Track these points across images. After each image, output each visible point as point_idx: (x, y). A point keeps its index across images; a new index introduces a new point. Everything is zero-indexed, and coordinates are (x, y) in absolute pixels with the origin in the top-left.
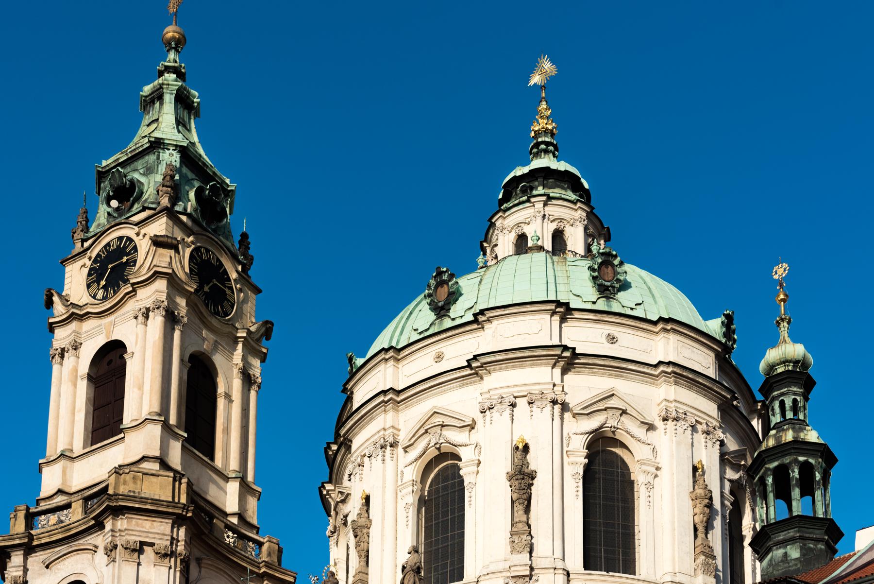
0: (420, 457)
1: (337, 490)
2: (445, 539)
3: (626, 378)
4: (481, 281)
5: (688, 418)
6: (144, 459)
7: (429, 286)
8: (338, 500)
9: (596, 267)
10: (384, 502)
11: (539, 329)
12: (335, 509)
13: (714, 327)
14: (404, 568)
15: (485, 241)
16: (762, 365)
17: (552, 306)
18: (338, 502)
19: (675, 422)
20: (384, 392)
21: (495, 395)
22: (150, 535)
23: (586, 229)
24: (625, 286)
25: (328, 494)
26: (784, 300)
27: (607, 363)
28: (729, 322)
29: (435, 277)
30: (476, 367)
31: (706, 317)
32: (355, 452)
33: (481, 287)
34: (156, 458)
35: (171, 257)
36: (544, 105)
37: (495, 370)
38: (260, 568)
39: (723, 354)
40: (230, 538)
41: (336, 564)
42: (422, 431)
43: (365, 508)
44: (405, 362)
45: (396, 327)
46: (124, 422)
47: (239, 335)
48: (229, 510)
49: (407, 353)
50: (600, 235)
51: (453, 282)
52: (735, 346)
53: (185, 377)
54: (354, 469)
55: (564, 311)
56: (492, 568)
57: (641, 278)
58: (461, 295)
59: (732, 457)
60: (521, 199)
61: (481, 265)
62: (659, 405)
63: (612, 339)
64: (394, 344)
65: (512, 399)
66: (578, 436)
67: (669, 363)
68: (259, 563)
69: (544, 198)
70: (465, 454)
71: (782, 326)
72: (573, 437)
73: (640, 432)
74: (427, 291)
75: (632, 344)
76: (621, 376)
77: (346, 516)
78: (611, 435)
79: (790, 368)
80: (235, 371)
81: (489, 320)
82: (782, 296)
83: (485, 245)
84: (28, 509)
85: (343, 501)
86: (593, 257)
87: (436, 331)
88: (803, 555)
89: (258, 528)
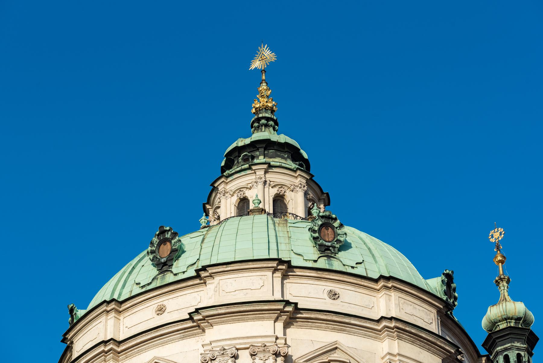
3: (349, 333)
4: (203, 239)
7: (152, 244)
9: (316, 228)
11: (261, 285)
13: (435, 285)
15: (208, 203)
16: (484, 322)
17: (274, 264)
20: (105, 342)
21: (217, 346)
23: (306, 194)
24: (345, 246)
26: (502, 262)
28: (449, 280)
29: (158, 235)
30: (198, 320)
31: (426, 277)
33: (204, 245)
36: (264, 86)
37: (217, 323)
39: (446, 311)
49: (128, 306)
50: (319, 200)
51: (175, 240)
52: (456, 303)
55: (286, 268)
57: (361, 239)
58: (184, 252)
60: (243, 167)
61: (204, 225)
62: (383, 358)
63: (334, 296)
64: (116, 297)
65: (234, 351)
67: (391, 319)
69: (265, 166)
71: (501, 285)
74: (149, 249)
75: (353, 300)
76: (344, 330)
79: (512, 324)
81: (211, 276)
82: (499, 258)
83: (208, 207)
86: (314, 220)
87: (158, 285)
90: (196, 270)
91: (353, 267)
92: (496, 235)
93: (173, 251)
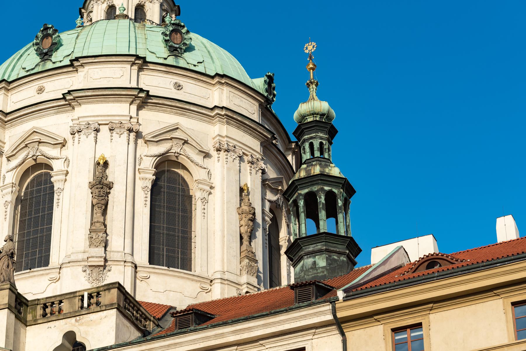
0: (20, 165)
2: (36, 232)
3: (189, 117)
4: (78, 36)
5: (237, 150)
7: (37, 37)
9: (168, 33)
11: (121, 75)
13: (259, 83)
15: (83, 8)
16: (296, 115)
17: (133, 59)
19: (226, 153)
24: (190, 49)
26: (313, 69)
27: (173, 104)
28: (270, 80)
29: (42, 31)
30: (69, 99)
31: (253, 76)
33: (78, 41)
37: (84, 103)
39: (265, 104)
42: (23, 145)
45: (9, 65)
49: (15, 85)
50: (172, 10)
51: (56, 36)
52: (274, 99)
55: (141, 63)
56: (73, 258)
57: (203, 43)
58: (62, 45)
59: (272, 183)
61: (79, 25)
62: (214, 139)
63: (178, 87)
64: (6, 78)
65: (97, 126)
66: (148, 158)
67: (223, 108)
70: (57, 165)
71: (311, 87)
72: (144, 158)
73: (198, 159)
74: (35, 41)
75: (193, 91)
78: (175, 159)
79: (318, 119)
81: (82, 65)
82: (311, 66)
83: (83, 11)
86: (166, 26)
87: (40, 70)
88: (329, 264)
90: (70, 60)
91: (195, 65)
92: (310, 48)
93: (53, 44)
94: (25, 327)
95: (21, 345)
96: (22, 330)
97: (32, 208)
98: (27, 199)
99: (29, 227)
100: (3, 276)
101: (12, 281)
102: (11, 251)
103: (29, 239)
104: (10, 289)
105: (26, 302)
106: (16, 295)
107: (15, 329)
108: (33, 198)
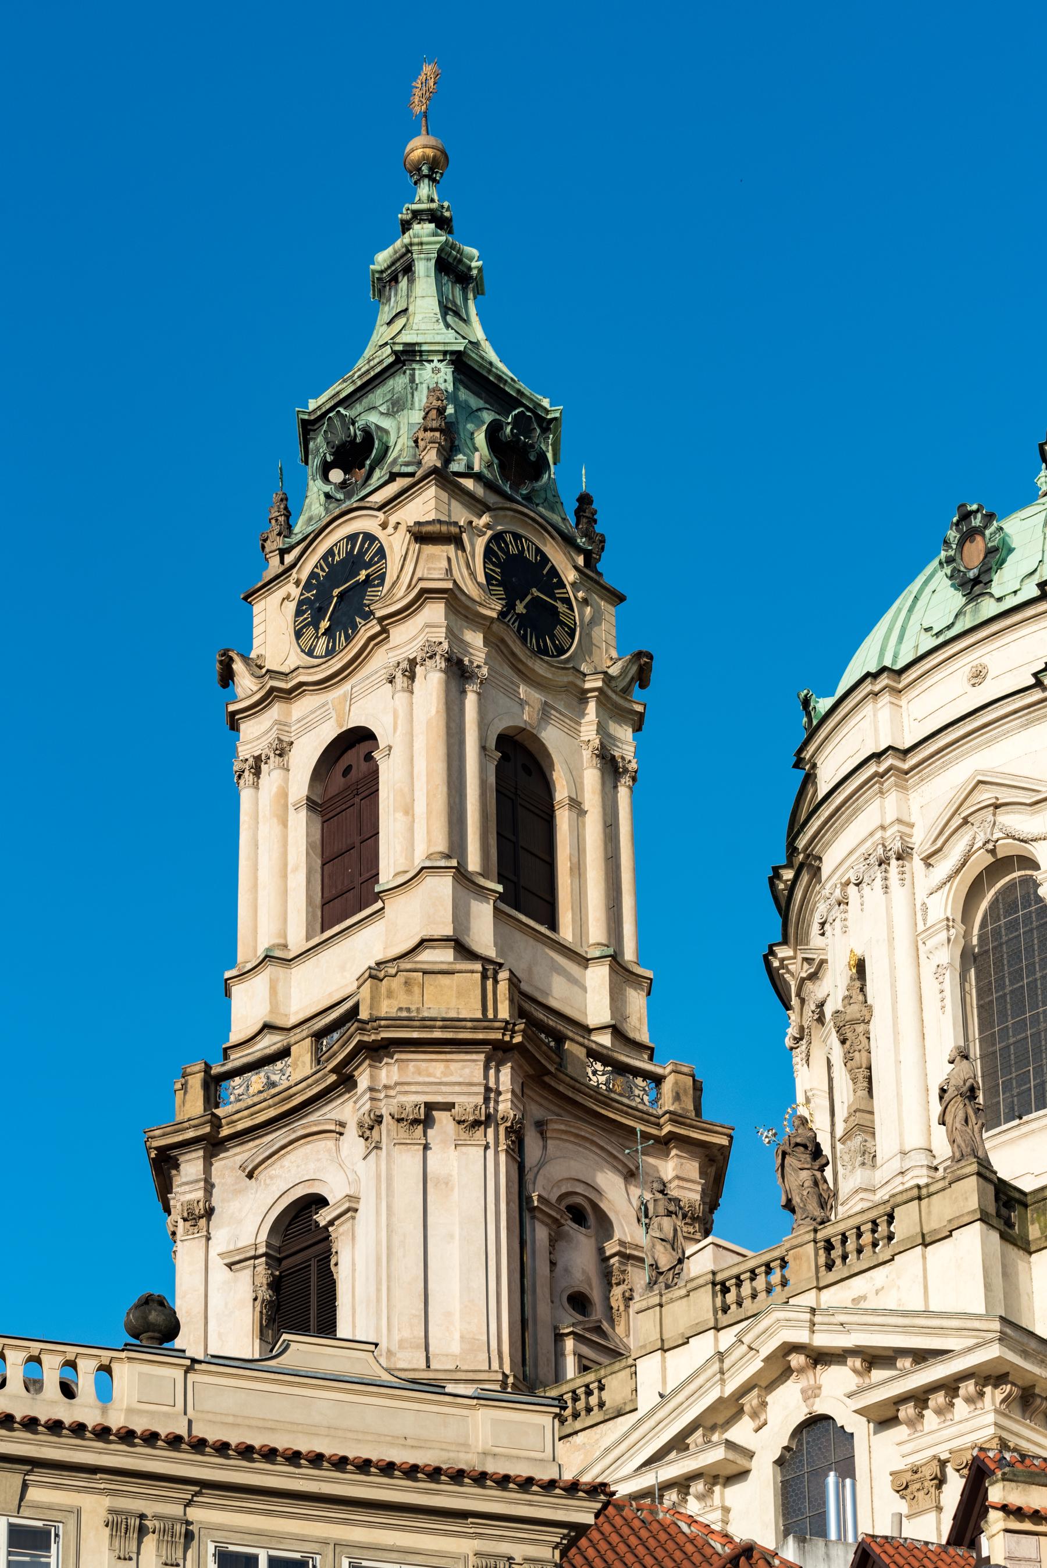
0: (958, 871)
1: (800, 956)
2: (1021, 1026)
6: (423, 943)
7: (947, 543)
8: (804, 975)
10: (893, 968)
12: (798, 995)
14: (943, 1091)
18: (803, 980)
20: (877, 756)
22: (444, 1089)
25: (782, 966)
29: (957, 524)
32: (829, 877)
34: (447, 939)
35: (449, 559)
38: (659, 1126)
40: (598, 1076)
41: (808, 1100)
42: (957, 821)
43: (858, 984)
44: (912, 693)
45: (890, 630)
46: (382, 878)
47: (588, 685)
48: (592, 1021)
53: (492, 779)
54: (829, 911)
58: (1011, 550)
64: (887, 663)
68: (659, 1118)
77: (821, 1005)
80: (587, 754)
84: (208, 1067)
85: (813, 977)
89: (652, 1049)
94: (1027, 1255)
95: (1024, 1299)
96: (1021, 1266)
97: (1003, 970)
98: (987, 951)
99: (1003, 1016)
100: (959, 1146)
101: (980, 1154)
102: (968, 1084)
103: (1008, 1047)
104: (979, 1174)
105: (1022, 1197)
106: (995, 1185)
107: (1004, 1266)
108: (1001, 945)
